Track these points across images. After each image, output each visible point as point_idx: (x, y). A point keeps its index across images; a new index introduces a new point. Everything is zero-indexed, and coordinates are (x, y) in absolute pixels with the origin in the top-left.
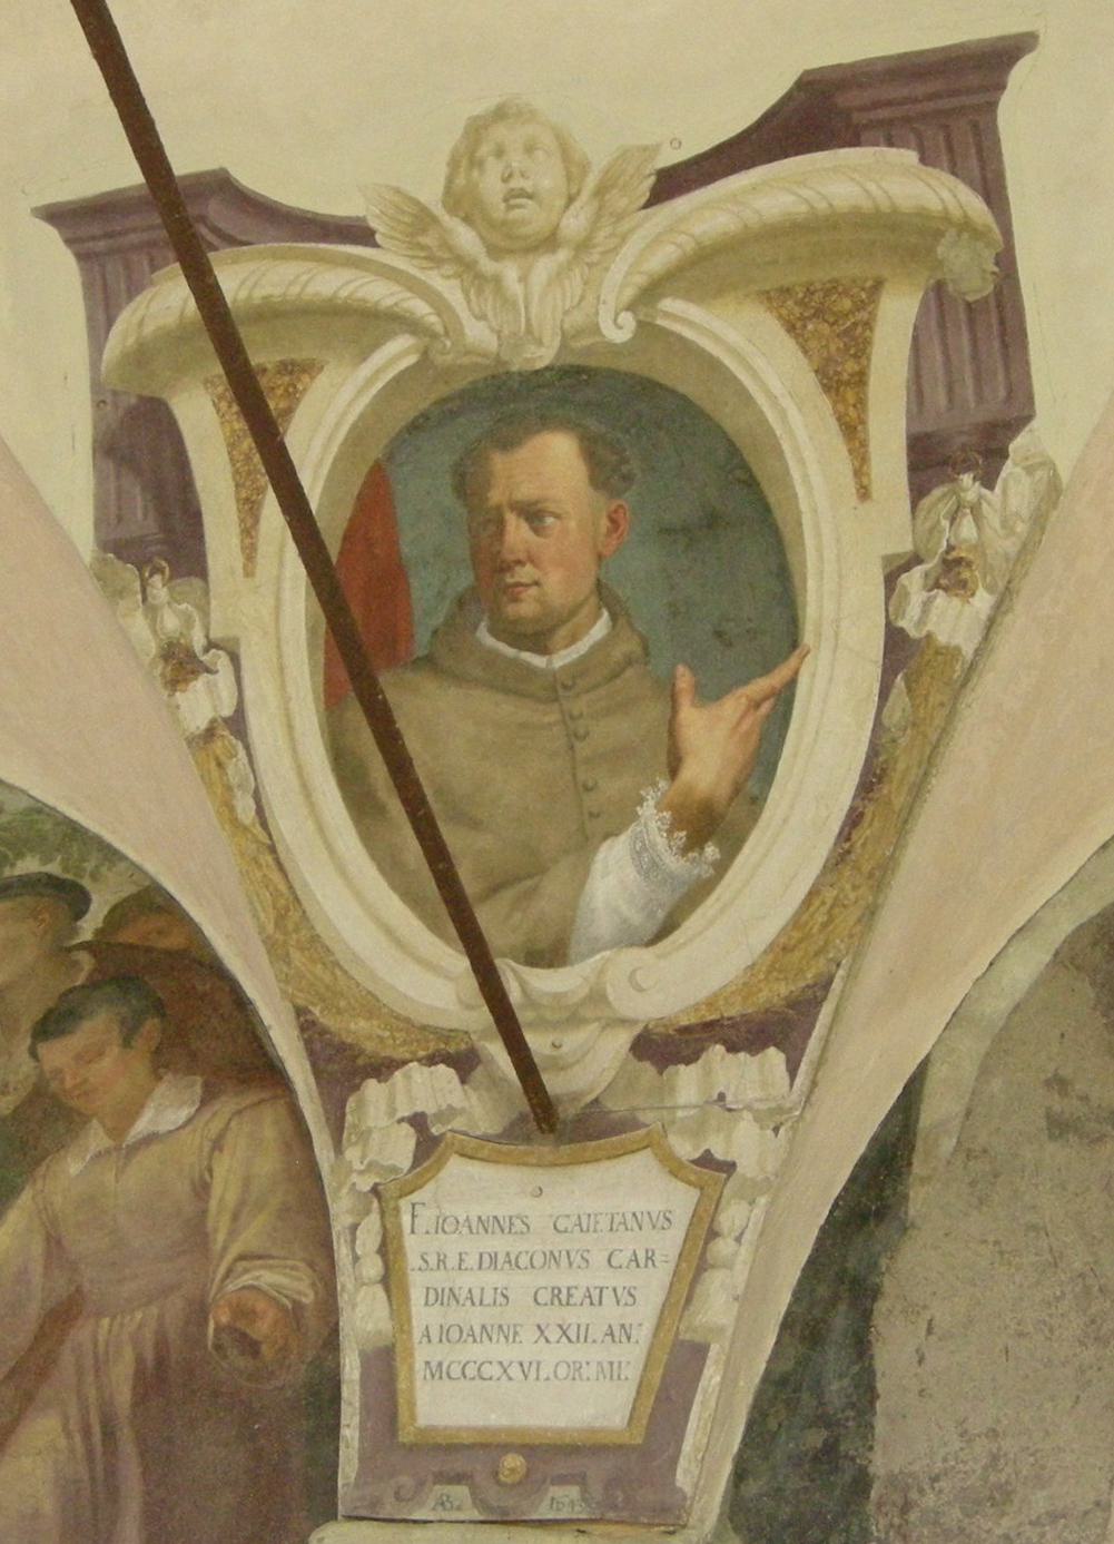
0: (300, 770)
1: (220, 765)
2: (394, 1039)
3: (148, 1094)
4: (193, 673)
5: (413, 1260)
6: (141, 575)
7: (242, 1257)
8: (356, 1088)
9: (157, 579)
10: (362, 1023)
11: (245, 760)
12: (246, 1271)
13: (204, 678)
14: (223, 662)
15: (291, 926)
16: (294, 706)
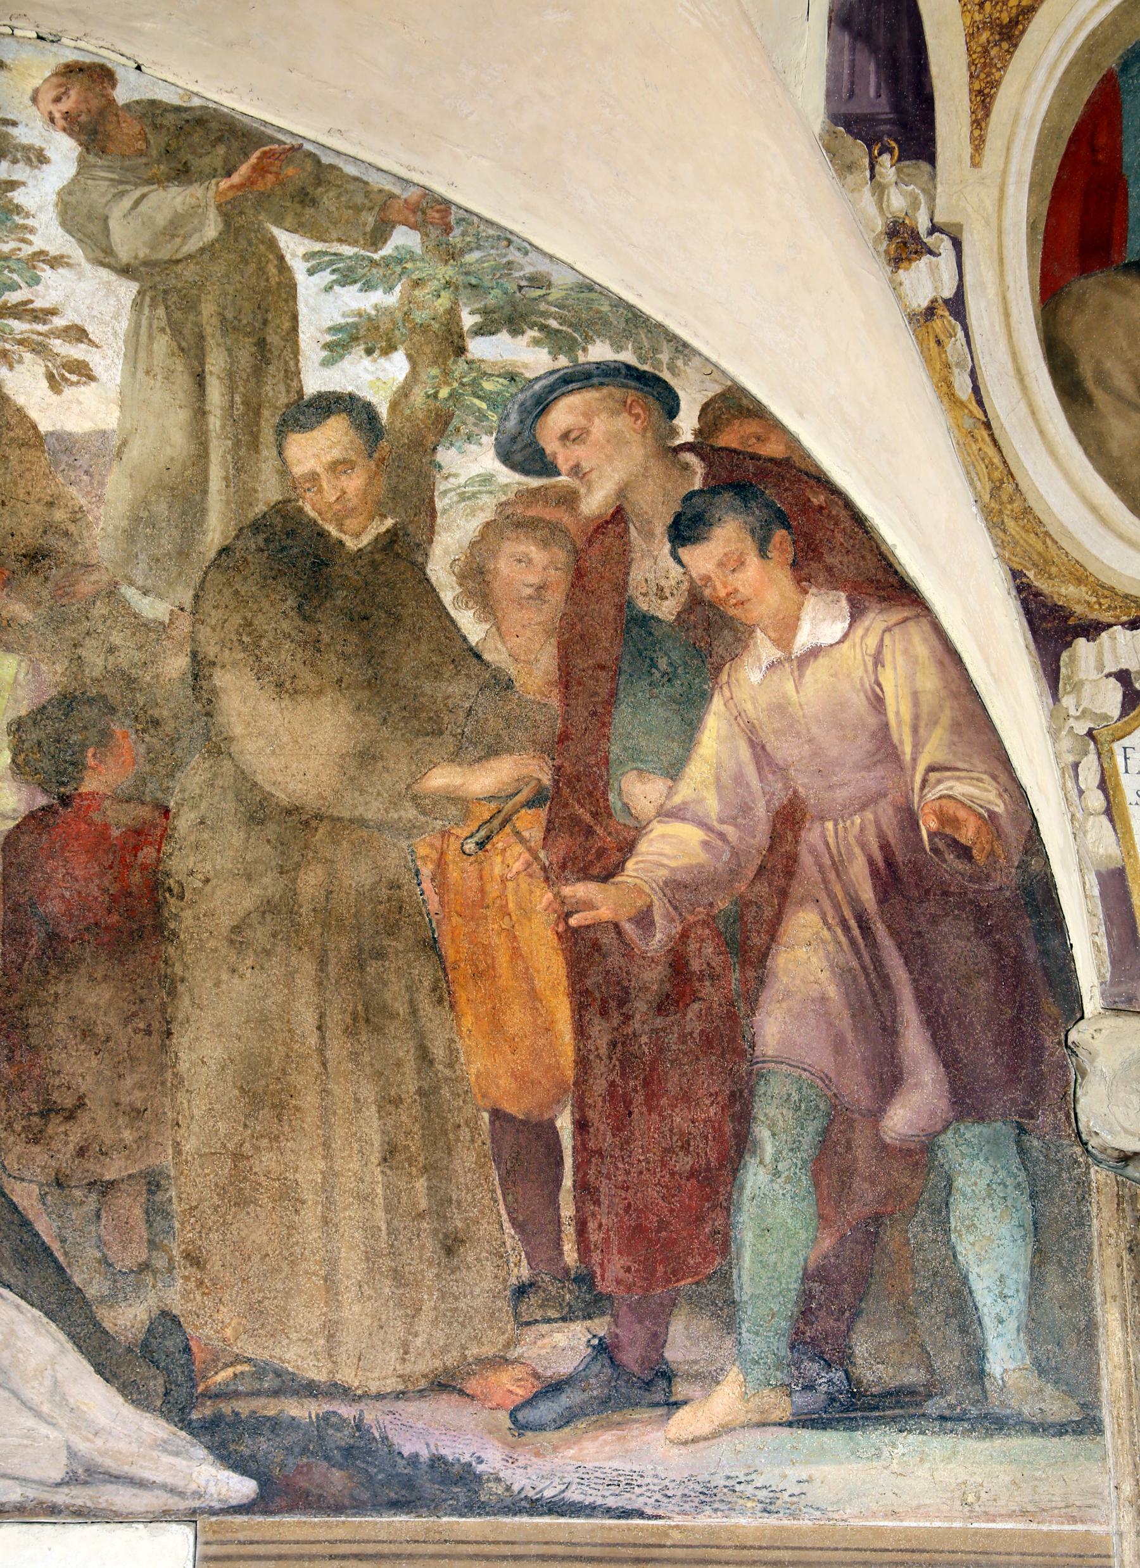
0: (1014, 355)
1: (939, 342)
2: (1100, 604)
3: (800, 606)
4: (916, 253)
5: (1130, 796)
6: (870, 153)
7: (931, 769)
8: (1069, 644)
9: (886, 159)
10: (1071, 588)
11: (964, 341)
12: (939, 782)
13: (926, 259)
14: (945, 246)
15: (1005, 498)
16: (1011, 295)
